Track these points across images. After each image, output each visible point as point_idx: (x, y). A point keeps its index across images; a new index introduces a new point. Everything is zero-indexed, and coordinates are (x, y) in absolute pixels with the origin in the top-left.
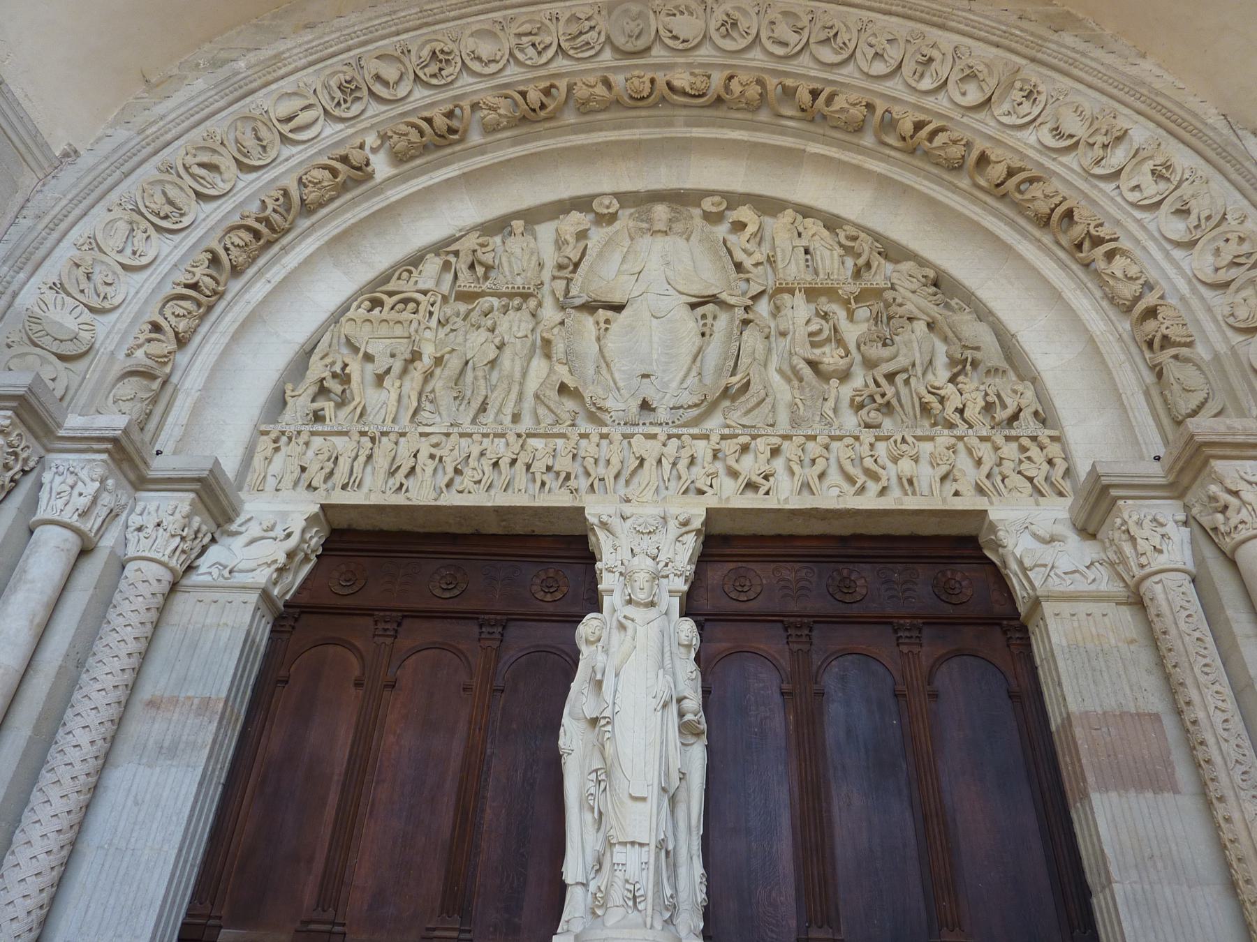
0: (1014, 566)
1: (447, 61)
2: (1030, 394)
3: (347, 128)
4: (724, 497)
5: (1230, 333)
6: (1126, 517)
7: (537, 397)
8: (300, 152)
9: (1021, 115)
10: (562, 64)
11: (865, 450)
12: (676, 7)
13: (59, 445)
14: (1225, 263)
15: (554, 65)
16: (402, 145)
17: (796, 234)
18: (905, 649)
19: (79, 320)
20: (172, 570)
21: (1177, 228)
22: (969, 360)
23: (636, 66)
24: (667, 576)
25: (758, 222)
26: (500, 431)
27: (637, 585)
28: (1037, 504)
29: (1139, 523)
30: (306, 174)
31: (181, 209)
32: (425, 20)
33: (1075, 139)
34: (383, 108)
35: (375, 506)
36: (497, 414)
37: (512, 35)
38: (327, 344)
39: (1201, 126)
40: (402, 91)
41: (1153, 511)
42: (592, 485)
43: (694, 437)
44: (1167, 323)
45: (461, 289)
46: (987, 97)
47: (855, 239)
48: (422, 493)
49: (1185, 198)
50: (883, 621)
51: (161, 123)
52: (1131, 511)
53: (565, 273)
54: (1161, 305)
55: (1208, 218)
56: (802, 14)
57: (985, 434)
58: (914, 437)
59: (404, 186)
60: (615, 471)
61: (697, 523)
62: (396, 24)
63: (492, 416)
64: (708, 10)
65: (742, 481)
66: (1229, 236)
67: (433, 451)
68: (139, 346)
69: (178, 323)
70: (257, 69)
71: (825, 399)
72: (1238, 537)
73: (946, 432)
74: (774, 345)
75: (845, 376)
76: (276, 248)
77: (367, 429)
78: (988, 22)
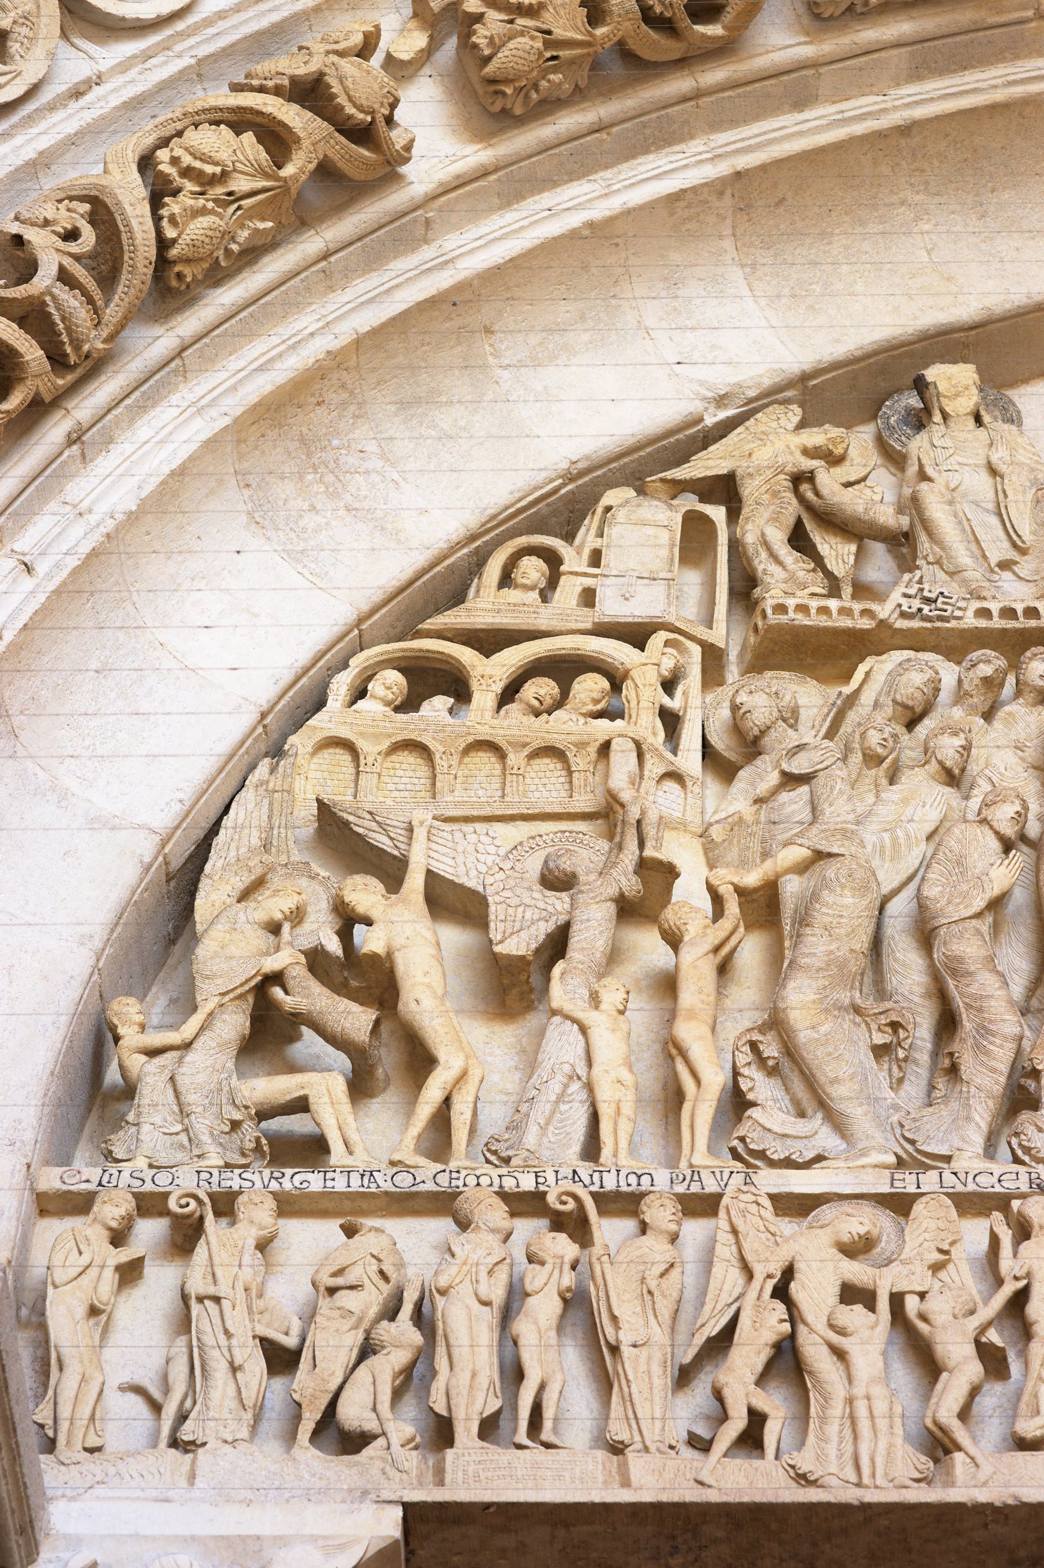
8: (123, 67)
30: (164, 142)
35: (658, 1507)
59: (509, 218)
67: (857, 1271)
77: (528, 1183)
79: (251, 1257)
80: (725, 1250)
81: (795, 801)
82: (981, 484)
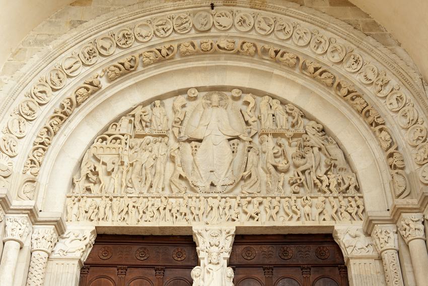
1: (129, 38)
2: (354, 179)
4: (242, 222)
5: (415, 165)
10: (175, 36)
11: (293, 203)
12: (220, 14)
13: (10, 211)
14: (416, 138)
16: (113, 75)
18: (305, 276)
20: (48, 253)
22: (333, 165)
23: (205, 36)
25: (254, 102)
27: (213, 257)
28: (352, 223)
29: (381, 233)
31: (34, 111)
32: (120, 21)
33: (372, 81)
34: (104, 59)
36: (156, 189)
37: (155, 26)
38: (87, 158)
39: (413, 83)
40: (111, 52)
42: (194, 218)
43: (231, 198)
44: (396, 160)
45: (138, 133)
46: (342, 59)
47: (293, 110)
50: (297, 266)
52: (378, 228)
53: (178, 125)
55: (412, 120)
58: (311, 197)
61: (233, 232)
63: (155, 189)
64: (234, 14)
65: (248, 215)
66: (418, 128)
67: (134, 204)
70: (57, 49)
71: (279, 182)
72: (409, 239)
73: (322, 195)
76: (67, 122)
81: (136, 154)
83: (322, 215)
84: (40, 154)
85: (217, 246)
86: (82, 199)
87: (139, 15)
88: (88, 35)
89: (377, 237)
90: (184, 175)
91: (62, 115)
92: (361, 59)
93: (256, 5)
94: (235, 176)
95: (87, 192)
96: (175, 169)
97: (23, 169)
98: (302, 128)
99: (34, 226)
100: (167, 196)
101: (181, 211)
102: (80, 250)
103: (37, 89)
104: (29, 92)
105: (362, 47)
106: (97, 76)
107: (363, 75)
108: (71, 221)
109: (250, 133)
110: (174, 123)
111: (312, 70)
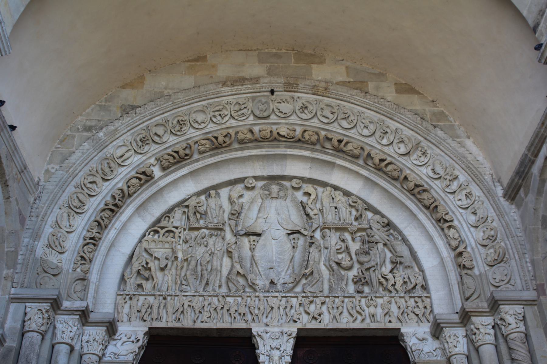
0: (409, 350)
2: (420, 278)
3: (143, 156)
4: (304, 323)
5: (485, 265)
6: (446, 334)
7: (228, 278)
9: (421, 161)
10: (233, 122)
11: (357, 303)
12: (281, 100)
15: (228, 123)
16: (166, 164)
17: (331, 198)
19: (57, 259)
21: (472, 219)
22: (399, 262)
23: (264, 123)
24: (284, 356)
26: (215, 295)
27: (274, 361)
28: (419, 325)
29: (450, 337)
32: (174, 107)
33: (440, 176)
34: (157, 146)
36: (213, 286)
39: (483, 180)
40: (165, 139)
41: (455, 332)
42: (253, 319)
44: (465, 260)
47: (356, 202)
48: (187, 323)
49: (476, 208)
51: (74, 166)
52: (447, 332)
54: (464, 252)
55: (482, 218)
56: (334, 107)
57: (402, 296)
58: (375, 297)
60: (262, 313)
61: (294, 335)
62: (162, 110)
63: (211, 288)
64: (295, 101)
65: (311, 316)
67: (189, 303)
68: (78, 267)
69: (90, 255)
72: (478, 344)
73: (388, 295)
74: (322, 252)
75: (350, 268)
76: (118, 214)
77: (161, 294)
78: (409, 120)
79: (136, 302)
80: (178, 301)
82: (214, 206)
83: (387, 316)
84: (90, 250)
85: (279, 349)
86: (133, 297)
87: (195, 100)
88: (141, 121)
89: (445, 341)
90: (242, 272)
91: (113, 208)
92: (428, 152)
93: (318, 92)
94: (296, 274)
95: (140, 290)
96: (232, 266)
97: (72, 266)
98: (365, 222)
99: (85, 328)
100: (224, 294)
101: (240, 311)
102: (132, 353)
103: (87, 179)
104: (79, 183)
105: (430, 139)
106: (150, 165)
107: (430, 168)
108: (122, 321)
109: (312, 226)
110: (230, 215)
111: (377, 161)
